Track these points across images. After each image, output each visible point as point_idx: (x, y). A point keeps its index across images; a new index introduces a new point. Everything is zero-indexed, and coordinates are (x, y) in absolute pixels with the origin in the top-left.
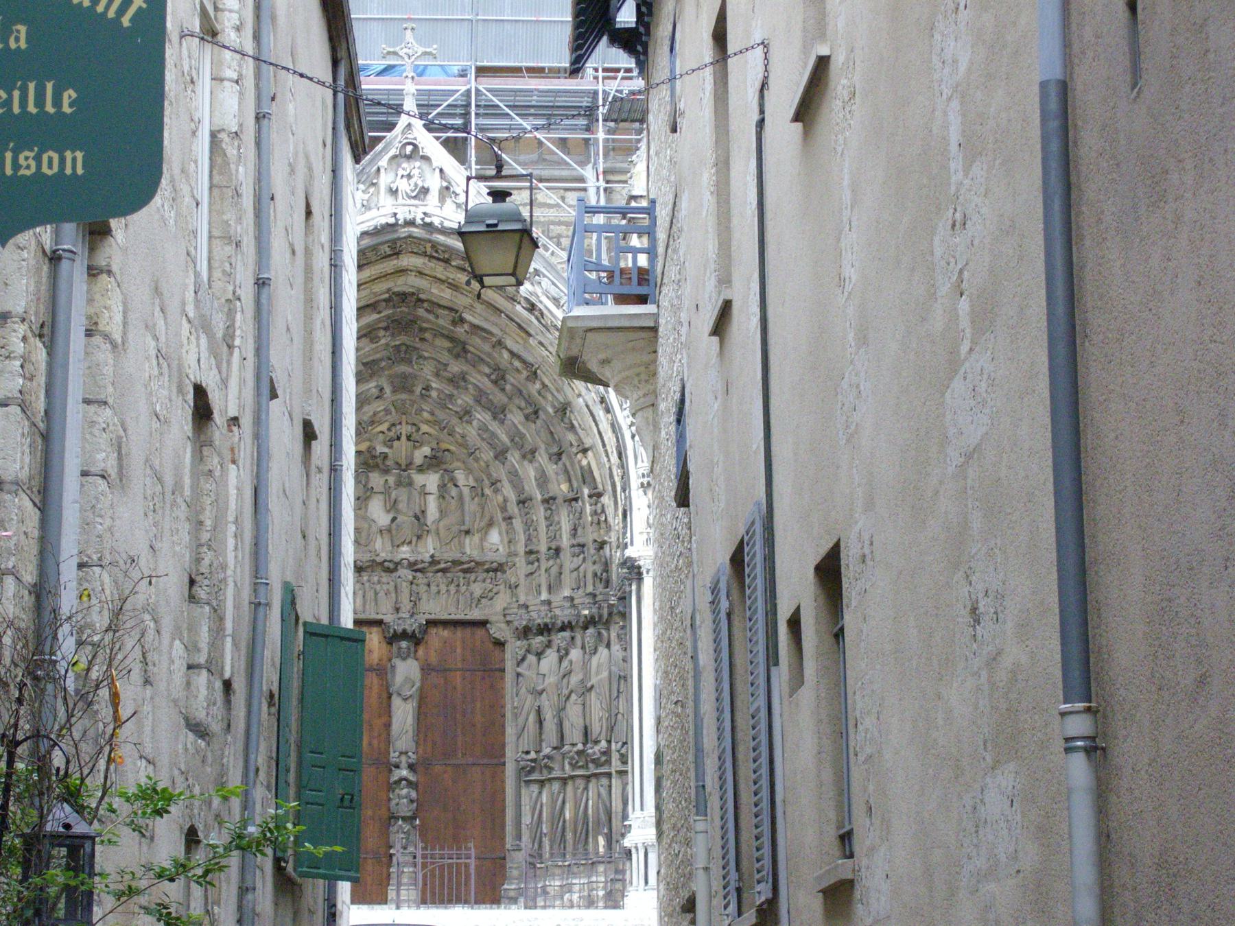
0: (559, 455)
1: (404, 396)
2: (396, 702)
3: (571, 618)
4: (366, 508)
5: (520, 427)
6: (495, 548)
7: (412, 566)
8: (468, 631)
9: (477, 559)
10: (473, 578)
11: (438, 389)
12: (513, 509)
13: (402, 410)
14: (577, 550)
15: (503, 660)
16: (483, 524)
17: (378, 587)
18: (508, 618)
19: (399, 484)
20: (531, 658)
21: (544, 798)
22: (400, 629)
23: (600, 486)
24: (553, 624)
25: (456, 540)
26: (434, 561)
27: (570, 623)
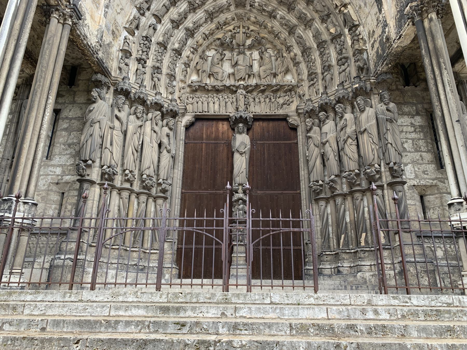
0: (328, 16)
1: (240, 11)
2: (236, 156)
3: (344, 94)
4: (222, 66)
5: (304, 11)
6: (290, 81)
7: (245, 88)
8: (276, 123)
9: (281, 84)
10: (278, 96)
11: (258, 2)
12: (300, 58)
13: (240, 18)
14: (343, 60)
15: (296, 137)
16: (283, 69)
17: (227, 100)
18: (300, 111)
19: (239, 53)
20: (316, 128)
21: (329, 210)
22: (238, 116)
23: (357, 23)
24: (331, 103)
25: (268, 77)
26: (257, 86)
27: (343, 97)
